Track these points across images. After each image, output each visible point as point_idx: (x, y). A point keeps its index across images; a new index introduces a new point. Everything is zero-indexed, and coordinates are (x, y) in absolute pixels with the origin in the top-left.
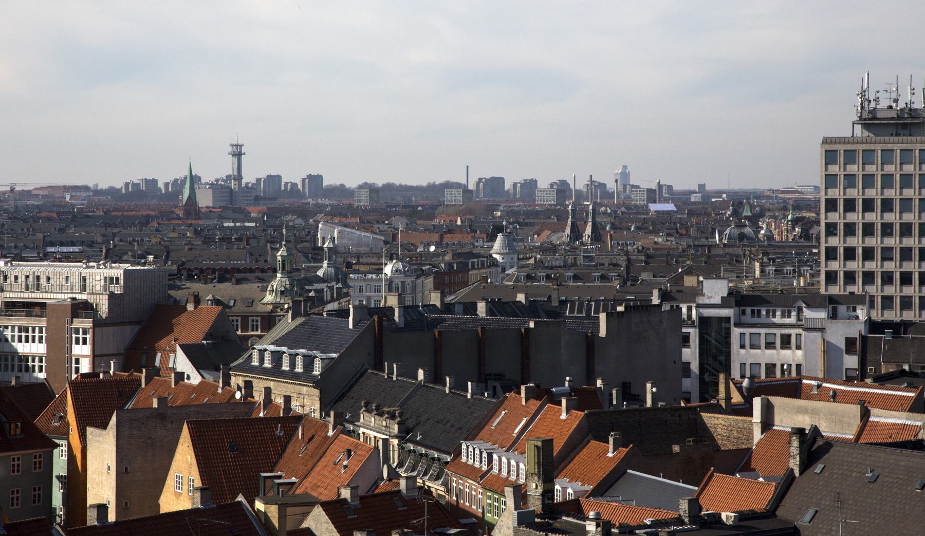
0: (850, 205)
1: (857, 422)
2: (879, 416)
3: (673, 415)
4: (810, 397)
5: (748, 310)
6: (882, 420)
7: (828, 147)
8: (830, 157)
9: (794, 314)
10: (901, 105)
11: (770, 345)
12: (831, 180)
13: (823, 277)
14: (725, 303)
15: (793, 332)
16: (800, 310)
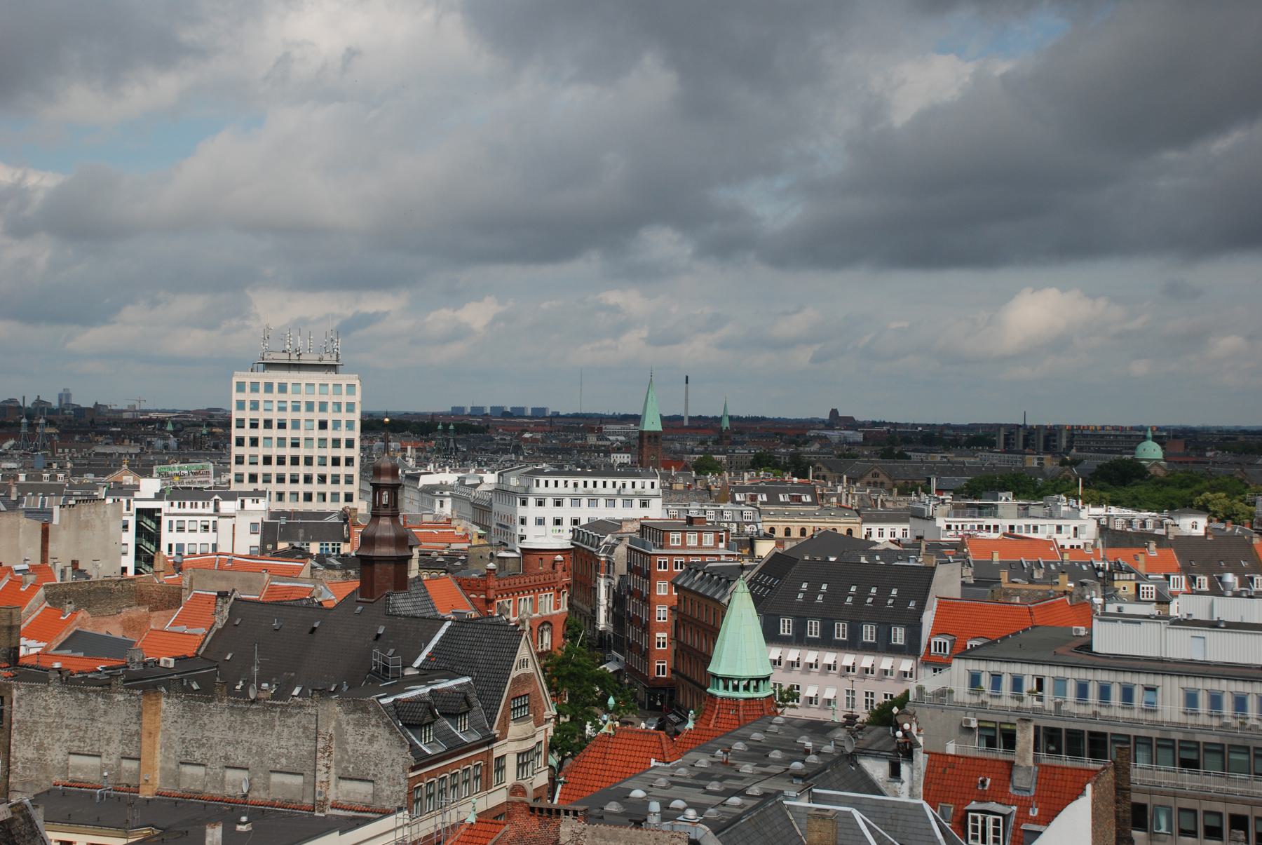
3: (116, 585)
5: (176, 503)
9: (212, 504)
14: (159, 497)
15: (211, 519)
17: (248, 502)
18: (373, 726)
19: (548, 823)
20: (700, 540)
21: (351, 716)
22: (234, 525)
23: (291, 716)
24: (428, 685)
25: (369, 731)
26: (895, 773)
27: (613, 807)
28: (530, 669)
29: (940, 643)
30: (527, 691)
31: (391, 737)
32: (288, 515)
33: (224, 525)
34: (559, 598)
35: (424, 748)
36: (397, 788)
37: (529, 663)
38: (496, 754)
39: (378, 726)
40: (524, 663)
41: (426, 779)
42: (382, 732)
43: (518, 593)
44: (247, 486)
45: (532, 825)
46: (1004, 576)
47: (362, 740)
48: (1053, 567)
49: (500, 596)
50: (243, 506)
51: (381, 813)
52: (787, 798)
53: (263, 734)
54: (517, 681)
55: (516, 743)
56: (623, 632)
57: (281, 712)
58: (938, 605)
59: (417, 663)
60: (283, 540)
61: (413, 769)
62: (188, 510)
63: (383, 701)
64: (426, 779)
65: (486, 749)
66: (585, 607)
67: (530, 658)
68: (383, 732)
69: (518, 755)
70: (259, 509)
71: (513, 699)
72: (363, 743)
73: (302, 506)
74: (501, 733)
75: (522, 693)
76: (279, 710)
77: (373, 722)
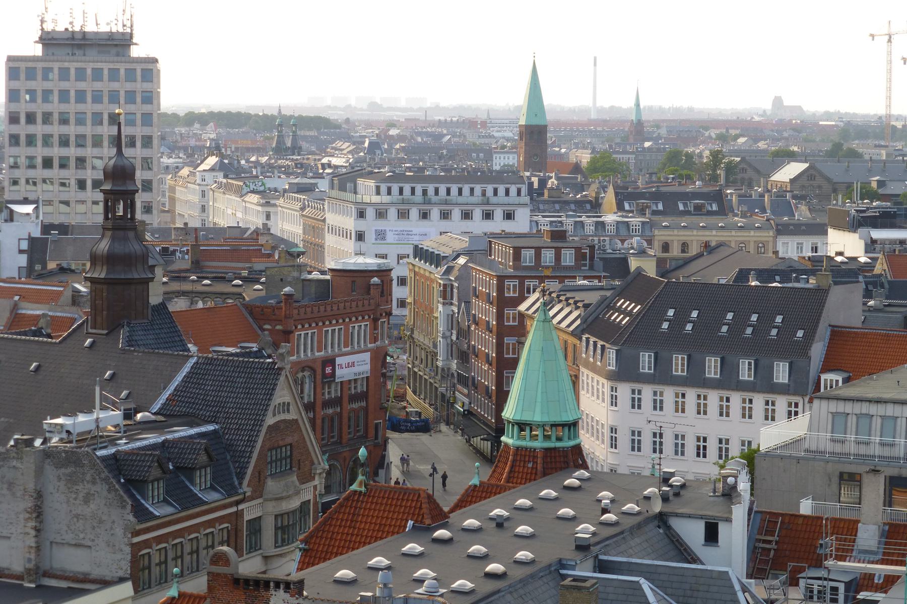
18: (88, 482)
19: (256, 597)
21: (63, 470)
24: (162, 434)
25: (83, 488)
26: (712, 535)
28: (292, 416)
29: (831, 381)
30: (289, 440)
31: (110, 496)
34: (375, 328)
35: (151, 509)
36: (119, 556)
37: (291, 407)
38: (247, 517)
39: (94, 482)
40: (286, 407)
41: (154, 545)
42: (99, 490)
43: (324, 324)
47: (75, 499)
49: (300, 327)
51: (100, 584)
54: (272, 428)
55: (273, 503)
56: (468, 370)
58: (831, 335)
59: (156, 407)
60: (52, 260)
63: (100, 453)
64: (154, 545)
65: (234, 509)
66: (426, 342)
68: (101, 488)
69: (276, 516)
71: (270, 450)
72: (78, 502)
74: (254, 491)
75: (281, 443)
77: (88, 477)
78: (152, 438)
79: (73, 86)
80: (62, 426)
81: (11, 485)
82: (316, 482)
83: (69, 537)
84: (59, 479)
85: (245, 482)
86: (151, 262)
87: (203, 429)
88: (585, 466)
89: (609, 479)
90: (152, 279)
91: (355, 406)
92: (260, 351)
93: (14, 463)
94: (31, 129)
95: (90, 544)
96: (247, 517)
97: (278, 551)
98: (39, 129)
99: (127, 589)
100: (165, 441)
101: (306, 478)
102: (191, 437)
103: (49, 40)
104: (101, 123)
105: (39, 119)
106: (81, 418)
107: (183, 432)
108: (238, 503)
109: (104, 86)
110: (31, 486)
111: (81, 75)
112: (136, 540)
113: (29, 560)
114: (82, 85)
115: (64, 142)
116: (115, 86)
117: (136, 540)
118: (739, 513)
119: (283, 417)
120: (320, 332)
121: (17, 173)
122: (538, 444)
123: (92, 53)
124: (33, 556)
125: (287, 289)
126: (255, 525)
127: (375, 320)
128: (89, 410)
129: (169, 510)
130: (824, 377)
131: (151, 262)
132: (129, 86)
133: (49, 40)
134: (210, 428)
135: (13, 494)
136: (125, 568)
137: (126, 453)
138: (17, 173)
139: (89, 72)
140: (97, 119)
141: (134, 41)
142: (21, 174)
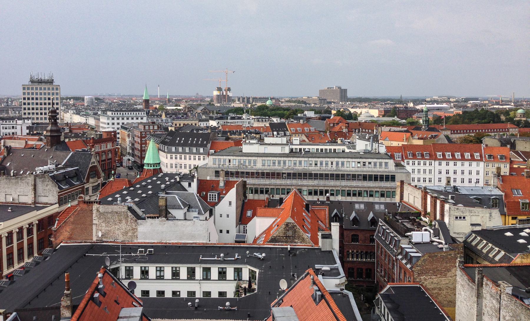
0: (29, 99)
1: (24, 144)
2: (30, 143)
4: (16, 139)
5: (4, 121)
6: (30, 143)
7: (23, 87)
8: (24, 89)
9: (15, 121)
10: (39, 78)
11: (10, 129)
12: (24, 94)
13: (23, 114)
15: (15, 125)
16: (16, 121)
17: (26, 121)
20: (153, 128)
22: (21, 127)
23: (24, 180)
26: (190, 185)
27: (110, 199)
28: (96, 164)
32: (37, 124)
33: (19, 127)
38: (85, 187)
39: (48, 182)
40: (94, 163)
44: (27, 116)
45: (85, 206)
46: (229, 134)
48: (241, 132)
50: (24, 122)
52: (159, 194)
53: (15, 185)
55: (91, 184)
56: (134, 152)
57: (20, 179)
59: (63, 164)
60: (35, 131)
61: (59, 193)
62: (8, 123)
66: (124, 146)
67: (95, 161)
68: (50, 183)
69: (92, 187)
70: (29, 122)
73: (39, 121)
76: (20, 178)
77: (47, 180)
78: (62, 171)
79: (39, 91)
80: (40, 169)
81: (28, 183)
82: (102, 178)
83: (43, 194)
84: (40, 181)
85: (85, 180)
86: (61, 131)
87: (75, 168)
88: (162, 173)
89: (166, 175)
90: (61, 135)
91: (109, 161)
92: (88, 150)
93: (29, 178)
94: (29, 101)
95: (47, 195)
96: (85, 188)
97: (93, 194)
98: (31, 101)
99: (57, 205)
100: (66, 171)
101: (99, 178)
102: (72, 170)
103: (32, 81)
104: (46, 100)
105: (31, 99)
106: (45, 167)
107: (70, 169)
108: (83, 184)
109: (47, 91)
110: (33, 183)
111: (41, 89)
112: (59, 194)
113: (33, 200)
114: (41, 91)
115: (37, 104)
116: (49, 91)
117: (59, 194)
118: (195, 180)
119: (93, 165)
120: (100, 146)
121: (25, 111)
122: (152, 168)
123: (43, 84)
124: (34, 199)
125: (92, 136)
126: (87, 189)
127: (113, 142)
128: (47, 165)
129: (67, 187)
130: (210, 151)
131: (61, 131)
132: (53, 91)
133: (32, 81)
134: (76, 168)
135: (28, 185)
136: (57, 201)
137: (56, 174)
138: (25, 111)
139: (43, 88)
140: (45, 99)
141: (54, 81)
142: (27, 111)
